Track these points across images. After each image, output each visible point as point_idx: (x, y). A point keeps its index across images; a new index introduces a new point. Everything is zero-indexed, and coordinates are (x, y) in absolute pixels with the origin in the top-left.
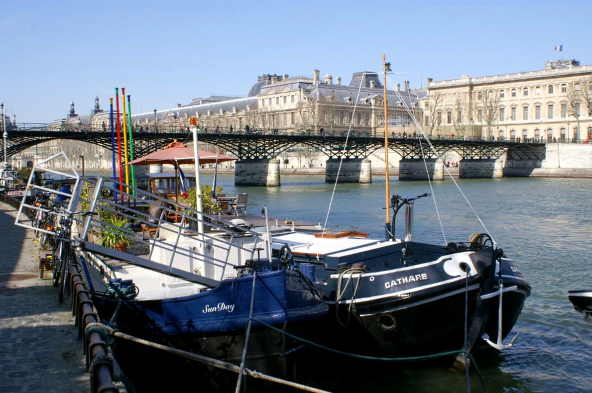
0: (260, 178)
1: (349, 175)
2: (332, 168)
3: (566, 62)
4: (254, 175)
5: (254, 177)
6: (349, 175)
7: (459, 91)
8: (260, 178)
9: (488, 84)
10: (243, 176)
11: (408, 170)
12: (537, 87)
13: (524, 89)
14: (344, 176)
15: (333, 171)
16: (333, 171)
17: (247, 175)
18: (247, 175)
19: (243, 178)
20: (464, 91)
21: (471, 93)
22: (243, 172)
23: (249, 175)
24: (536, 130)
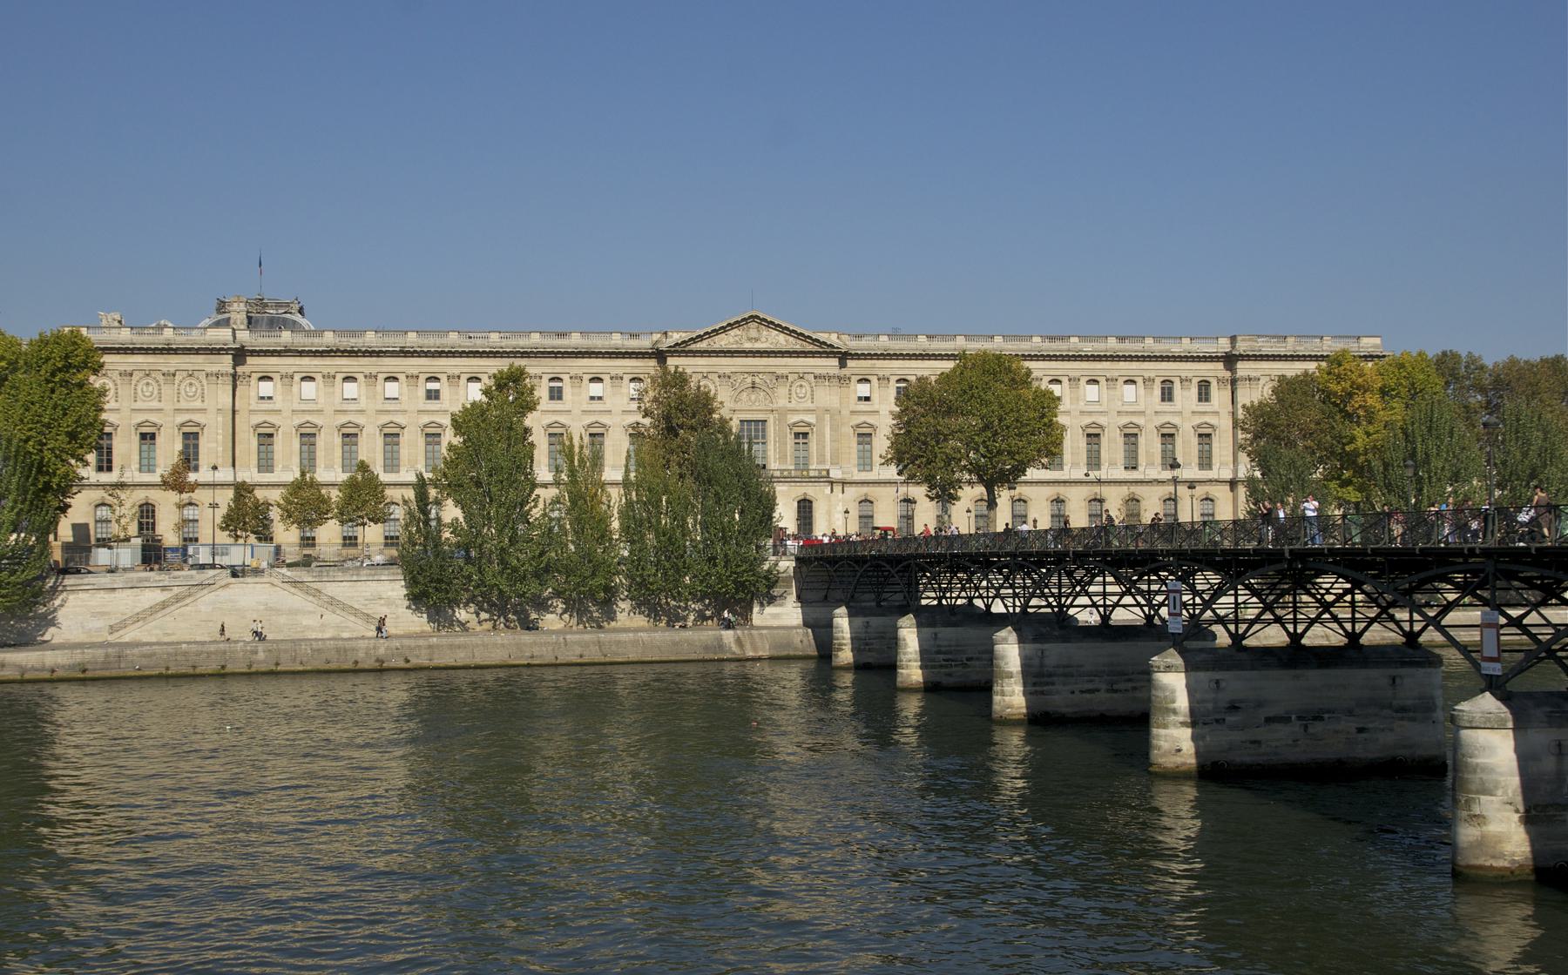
0: (1360, 730)
1: (1135, 688)
2: (1042, 665)
3: (279, 305)
4: (1318, 718)
5: (1317, 728)
6: (1135, 688)
7: (190, 367)
8: (1360, 730)
9: (301, 353)
10: (1233, 728)
11: (950, 652)
12: (346, 379)
13: (429, 379)
14: (1108, 691)
15: (1050, 675)
16: (1050, 675)
17: (1269, 720)
18: (1269, 720)
19: (1237, 737)
20: (215, 369)
21: (235, 377)
22: (1233, 708)
23: (1285, 719)
24: (97, 506)
